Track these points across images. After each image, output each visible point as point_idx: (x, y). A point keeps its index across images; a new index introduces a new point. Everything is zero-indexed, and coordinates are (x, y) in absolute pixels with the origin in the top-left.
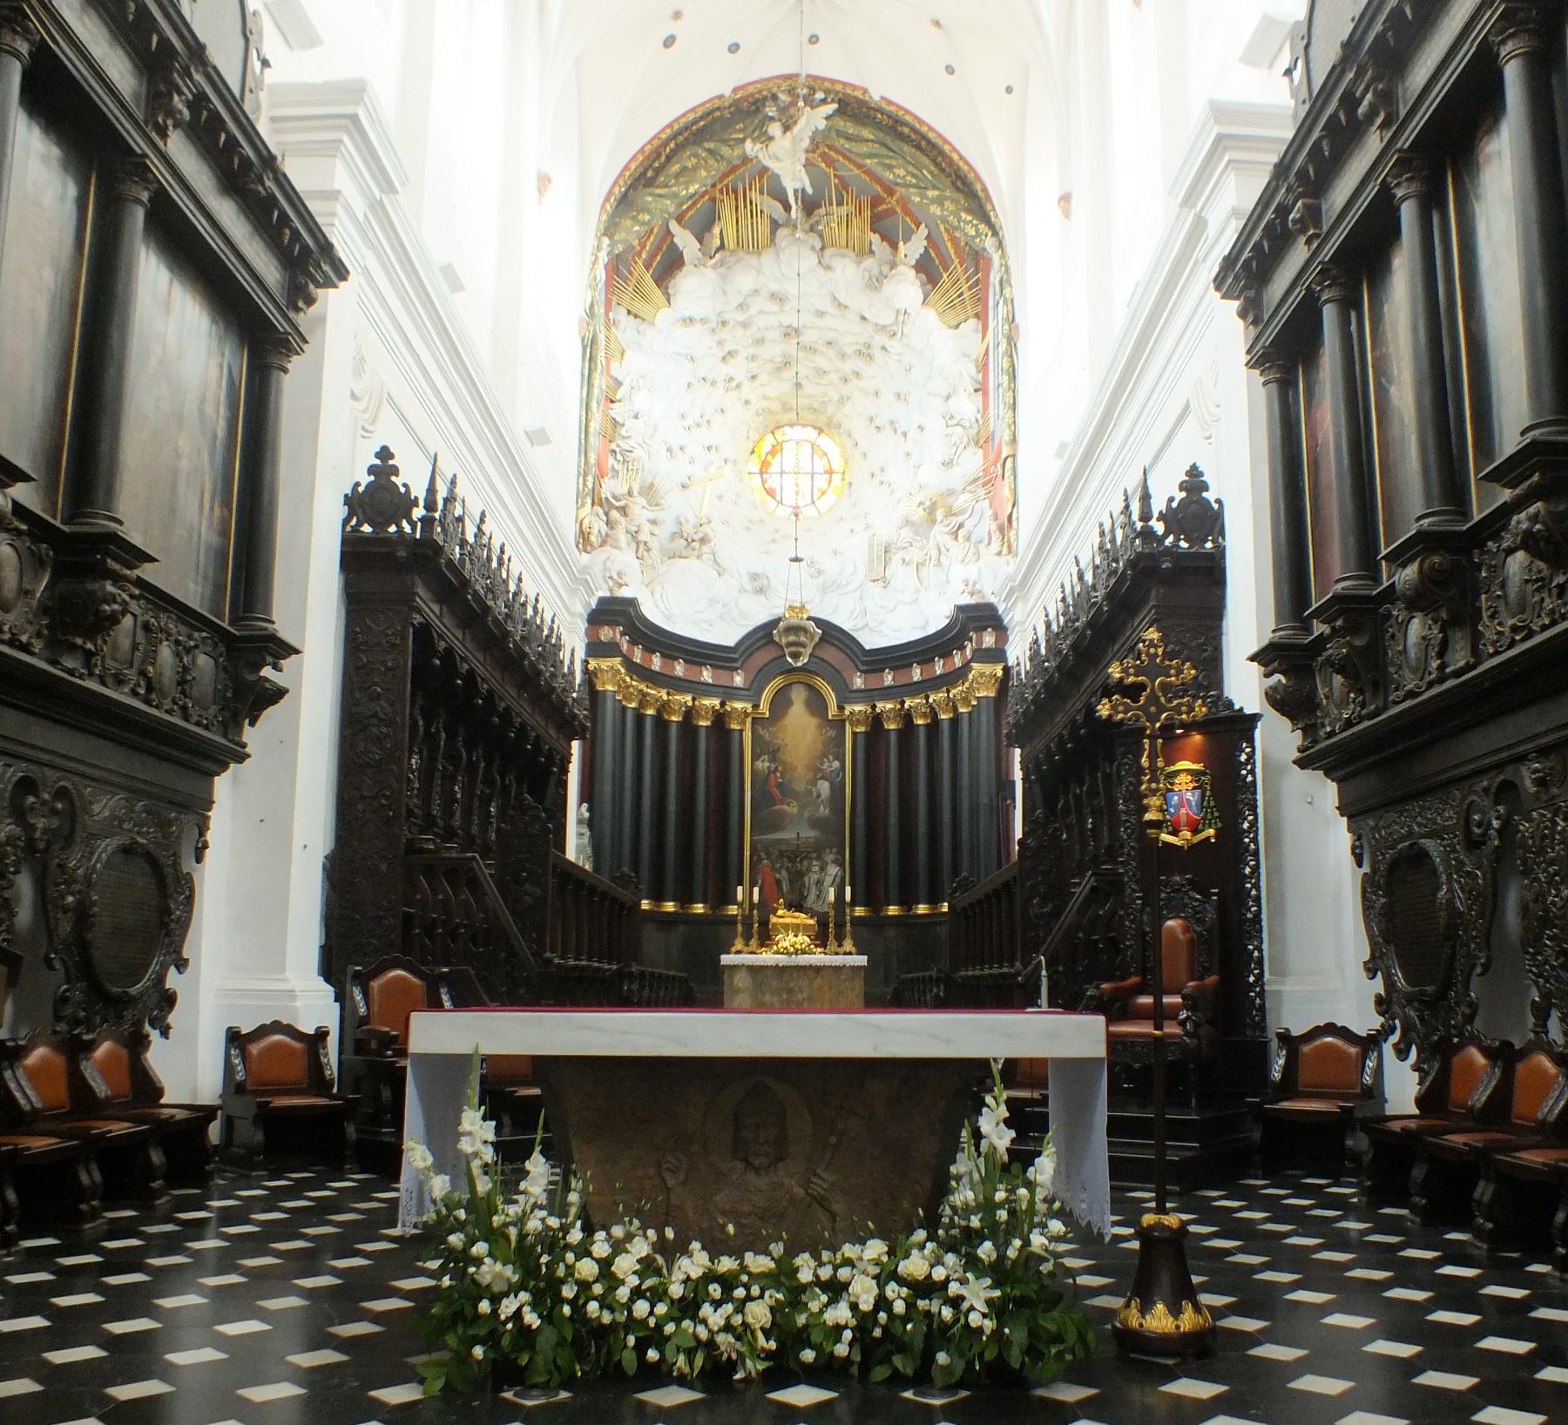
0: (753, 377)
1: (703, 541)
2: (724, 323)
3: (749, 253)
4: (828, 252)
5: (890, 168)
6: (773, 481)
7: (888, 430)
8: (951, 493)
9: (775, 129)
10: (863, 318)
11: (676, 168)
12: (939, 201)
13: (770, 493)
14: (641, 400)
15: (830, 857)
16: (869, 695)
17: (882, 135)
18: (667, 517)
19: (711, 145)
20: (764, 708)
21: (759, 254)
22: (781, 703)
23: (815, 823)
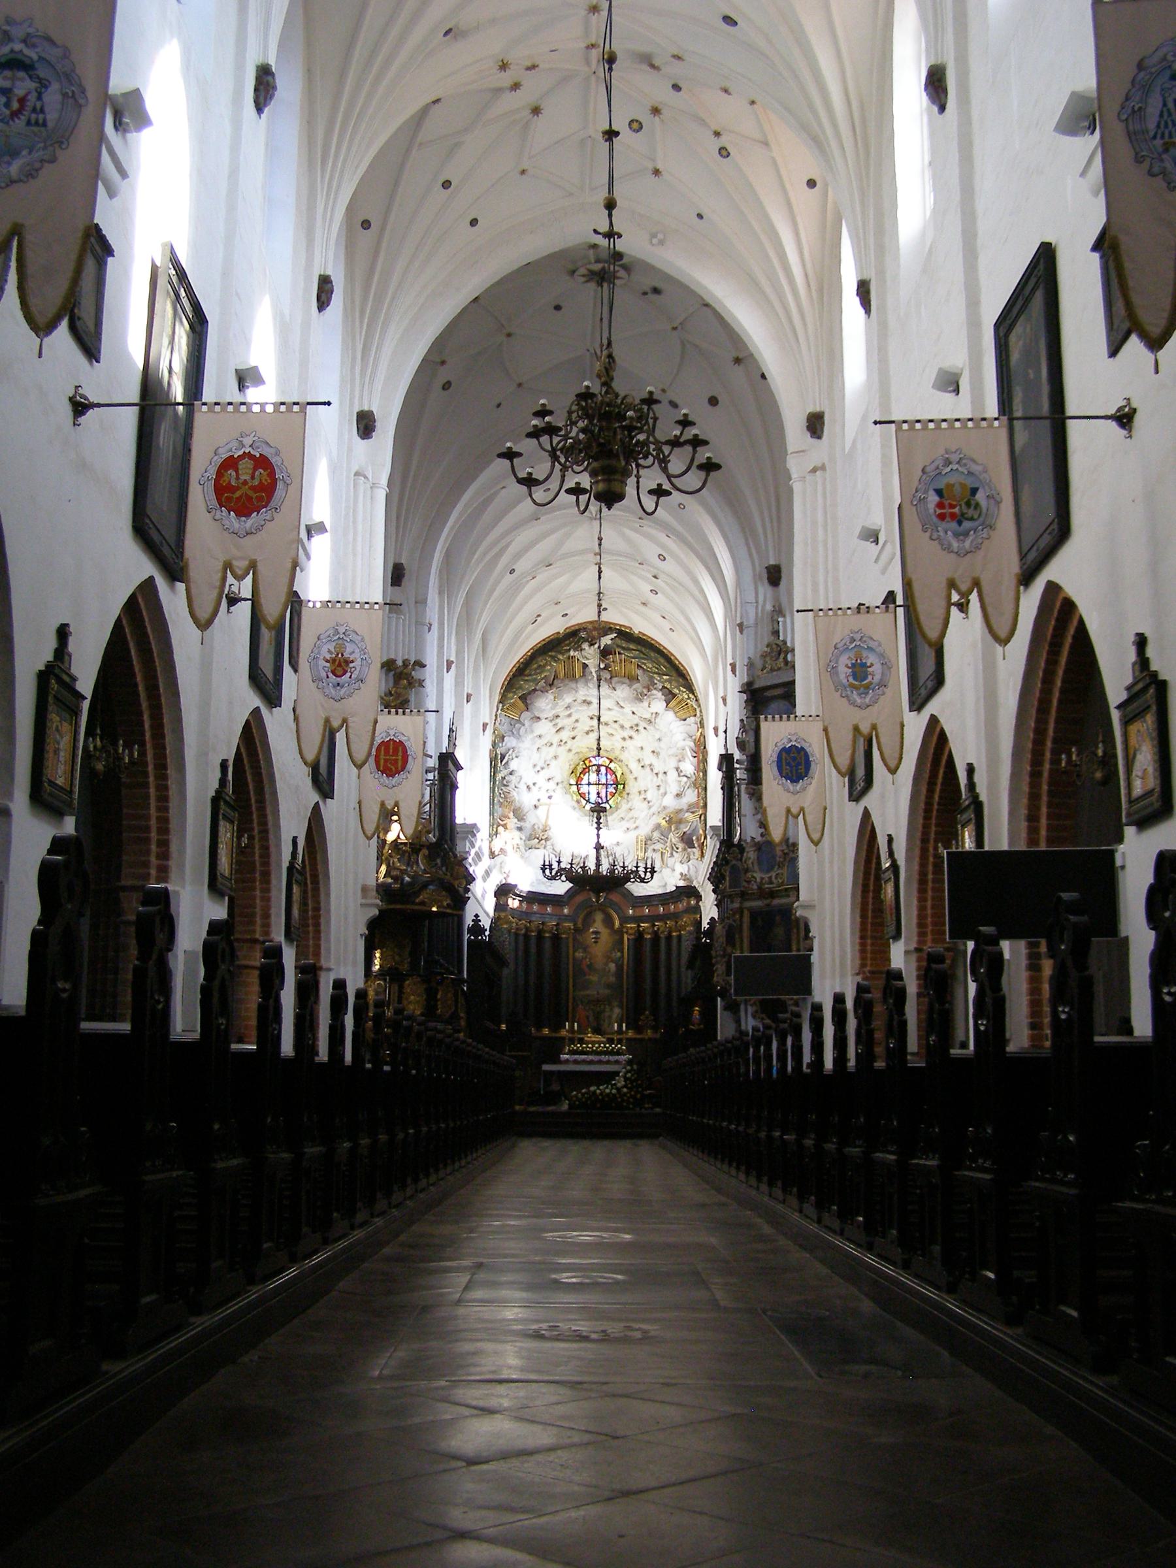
0: (573, 738)
1: (547, 840)
2: (558, 716)
3: (571, 680)
4: (615, 679)
5: (645, 664)
6: (584, 789)
7: (648, 769)
8: (681, 810)
9: (585, 646)
10: (633, 713)
11: (535, 666)
12: (669, 681)
13: (582, 795)
14: (513, 765)
15: (616, 1004)
16: (638, 919)
17: (639, 647)
18: (527, 825)
19: (553, 654)
20: (580, 925)
21: (577, 682)
22: (588, 920)
23: (608, 986)
